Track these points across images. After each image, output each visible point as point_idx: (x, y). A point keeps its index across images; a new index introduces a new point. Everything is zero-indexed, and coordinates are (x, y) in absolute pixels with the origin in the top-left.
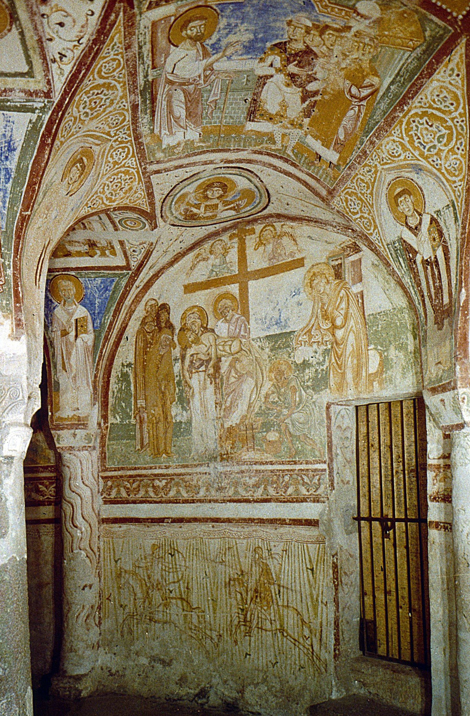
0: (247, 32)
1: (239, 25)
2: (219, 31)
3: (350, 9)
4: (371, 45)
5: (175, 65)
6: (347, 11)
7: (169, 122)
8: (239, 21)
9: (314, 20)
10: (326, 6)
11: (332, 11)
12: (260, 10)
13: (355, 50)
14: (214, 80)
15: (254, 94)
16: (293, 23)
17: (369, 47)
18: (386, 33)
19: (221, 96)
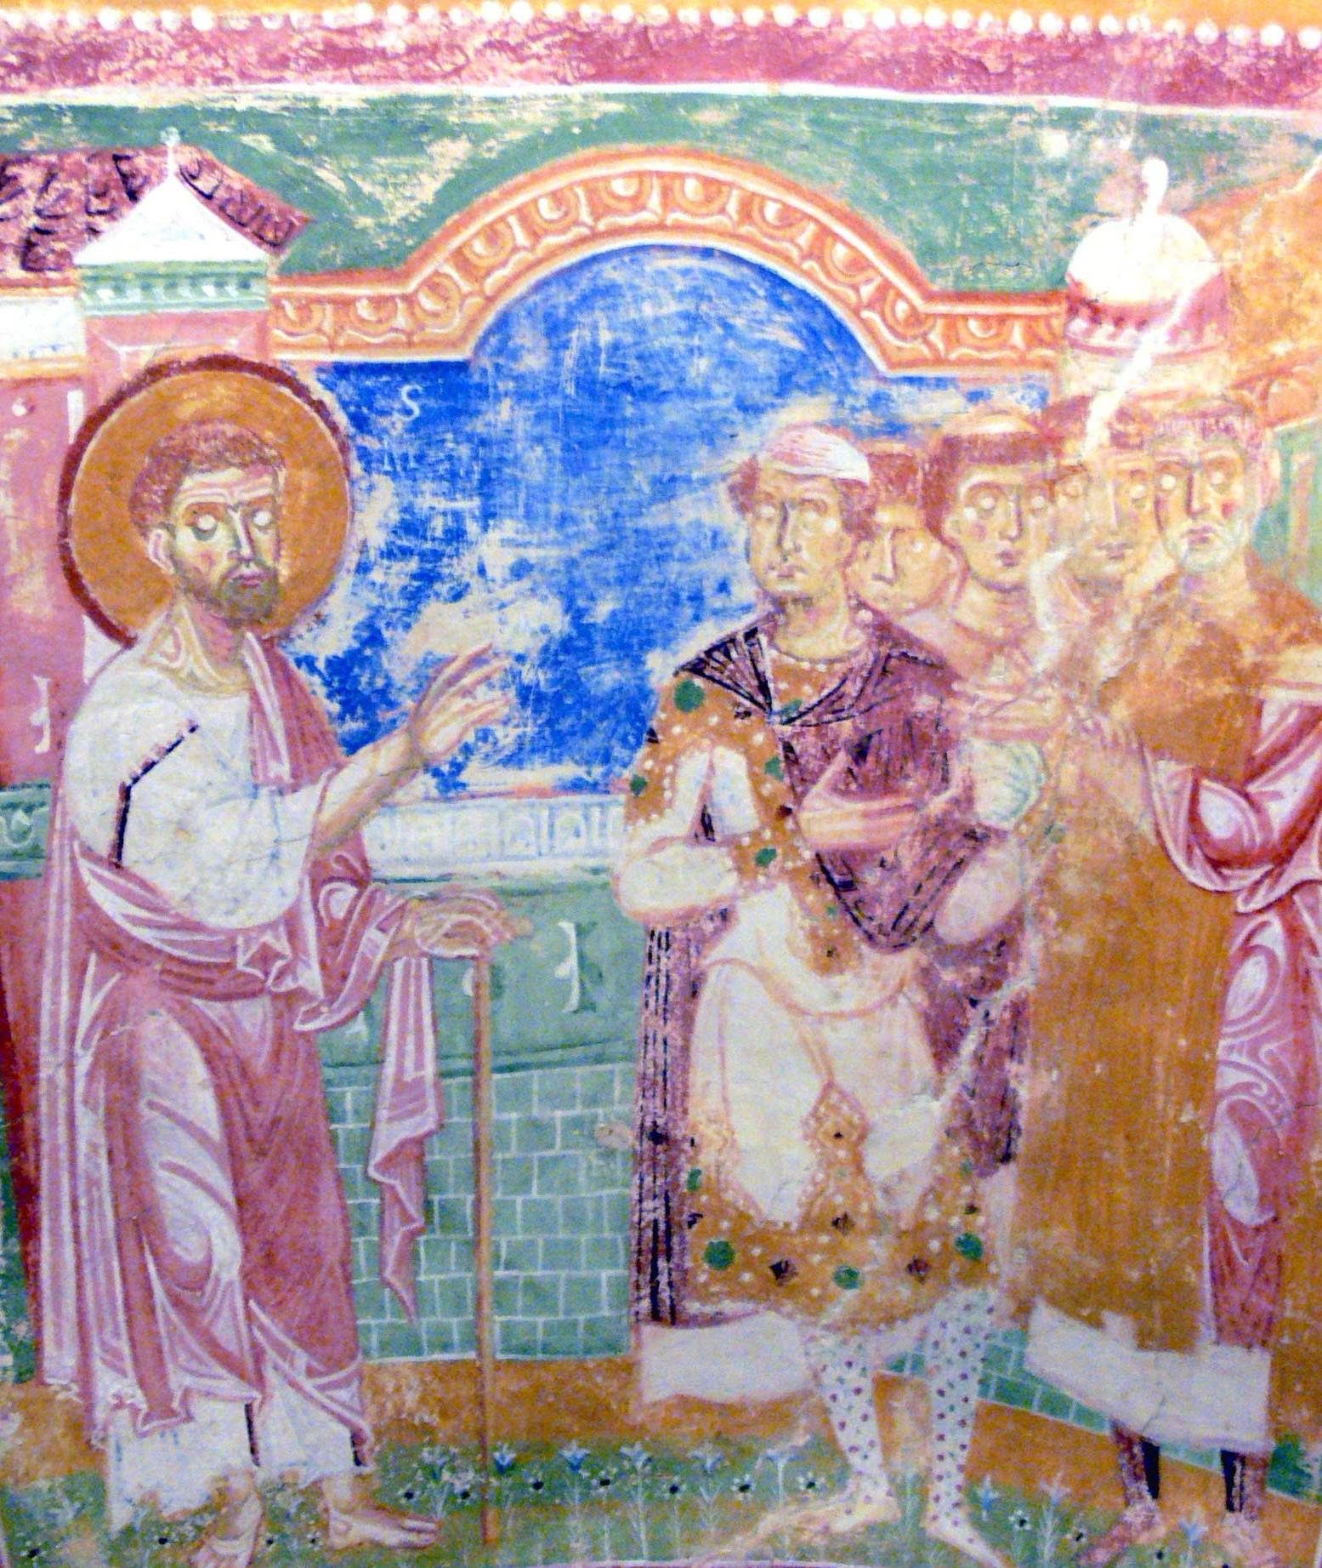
0: (526, 584)
1: (472, 528)
2: (363, 568)
3: (1045, 299)
4: (1220, 464)
5: (126, 793)
6: (1032, 318)
7: (138, 1306)
8: (469, 505)
9: (874, 433)
10: (915, 318)
11: (952, 338)
12: (569, 420)
13: (1150, 528)
14: (386, 965)
15: (646, 1085)
16: (765, 485)
17: (1218, 477)
18: (1280, 348)
19: (442, 1095)
